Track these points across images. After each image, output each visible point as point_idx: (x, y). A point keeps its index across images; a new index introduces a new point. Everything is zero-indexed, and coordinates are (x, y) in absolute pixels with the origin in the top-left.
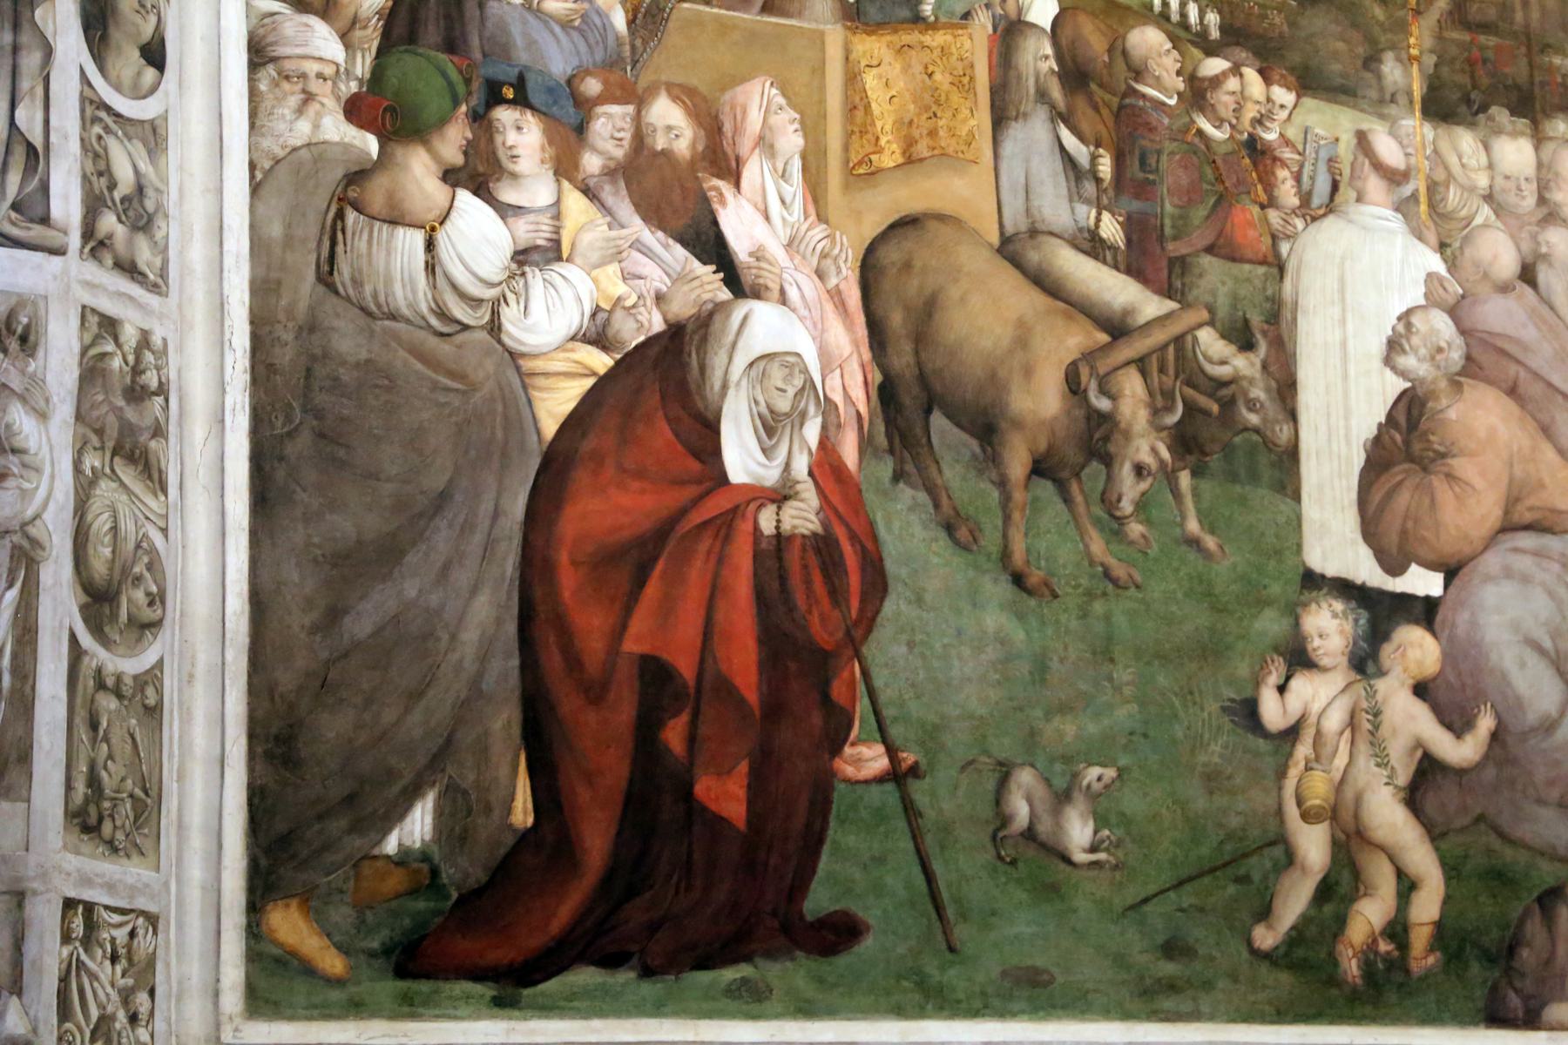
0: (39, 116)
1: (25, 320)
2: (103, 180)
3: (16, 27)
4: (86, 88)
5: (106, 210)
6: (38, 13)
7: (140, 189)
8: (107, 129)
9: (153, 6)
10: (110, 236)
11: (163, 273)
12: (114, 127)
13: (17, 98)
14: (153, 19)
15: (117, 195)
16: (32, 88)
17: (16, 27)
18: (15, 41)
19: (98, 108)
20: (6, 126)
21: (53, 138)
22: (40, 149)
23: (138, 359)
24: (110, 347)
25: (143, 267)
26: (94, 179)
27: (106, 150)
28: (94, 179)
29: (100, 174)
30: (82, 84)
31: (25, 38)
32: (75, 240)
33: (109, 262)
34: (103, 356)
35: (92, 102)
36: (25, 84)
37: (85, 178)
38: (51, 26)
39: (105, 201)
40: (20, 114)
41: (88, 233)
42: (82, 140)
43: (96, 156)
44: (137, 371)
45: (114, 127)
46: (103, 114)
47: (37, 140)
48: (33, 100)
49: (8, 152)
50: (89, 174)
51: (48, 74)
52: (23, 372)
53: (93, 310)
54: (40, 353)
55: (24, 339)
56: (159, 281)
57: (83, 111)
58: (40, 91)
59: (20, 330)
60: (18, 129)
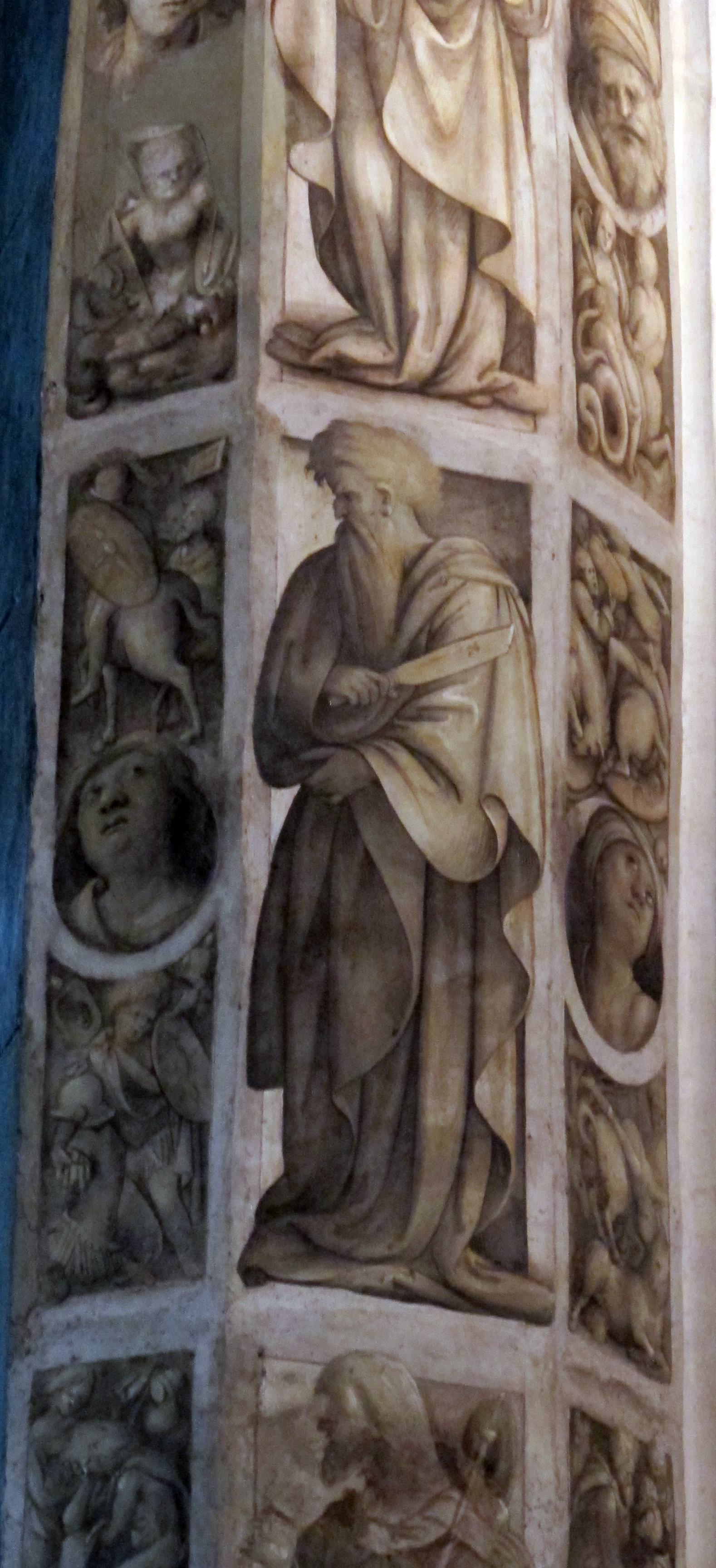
0: (510, 1091)
1: (491, 1434)
2: (593, 1192)
3: (475, 945)
4: (572, 1041)
5: (597, 1243)
6: (508, 919)
7: (635, 1204)
8: (596, 1108)
9: (649, 894)
10: (602, 1288)
11: (664, 1348)
12: (602, 1100)
13: (477, 1064)
14: (648, 914)
15: (609, 1217)
16: (500, 1046)
17: (475, 945)
18: (474, 968)
19: (585, 1073)
20: (462, 1110)
21: (531, 1128)
22: (511, 1146)
23: (637, 1498)
24: (604, 1477)
25: (641, 1336)
26: (583, 1192)
27: (594, 1140)
28: (583, 1192)
29: (590, 1184)
30: (567, 1036)
31: (490, 962)
32: (562, 1298)
33: (601, 1331)
34: (598, 1490)
35: (579, 1063)
36: (489, 1040)
37: (573, 1194)
38: (526, 939)
39: (595, 1227)
40: (483, 1089)
41: (578, 1286)
42: (568, 1129)
43: (585, 1153)
44: (637, 1515)
45: (602, 1100)
46: (590, 1082)
47: (507, 1131)
48: (500, 1067)
49: (464, 1153)
50: (577, 1185)
51: (523, 1024)
52: (489, 1521)
53: (584, 1415)
54: (516, 1492)
55: (490, 1467)
56: (661, 1358)
57: (568, 1079)
58: (510, 1049)
59: (483, 1452)
60: (480, 1116)
